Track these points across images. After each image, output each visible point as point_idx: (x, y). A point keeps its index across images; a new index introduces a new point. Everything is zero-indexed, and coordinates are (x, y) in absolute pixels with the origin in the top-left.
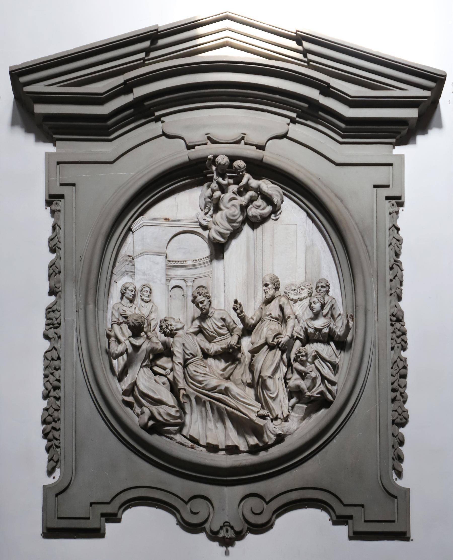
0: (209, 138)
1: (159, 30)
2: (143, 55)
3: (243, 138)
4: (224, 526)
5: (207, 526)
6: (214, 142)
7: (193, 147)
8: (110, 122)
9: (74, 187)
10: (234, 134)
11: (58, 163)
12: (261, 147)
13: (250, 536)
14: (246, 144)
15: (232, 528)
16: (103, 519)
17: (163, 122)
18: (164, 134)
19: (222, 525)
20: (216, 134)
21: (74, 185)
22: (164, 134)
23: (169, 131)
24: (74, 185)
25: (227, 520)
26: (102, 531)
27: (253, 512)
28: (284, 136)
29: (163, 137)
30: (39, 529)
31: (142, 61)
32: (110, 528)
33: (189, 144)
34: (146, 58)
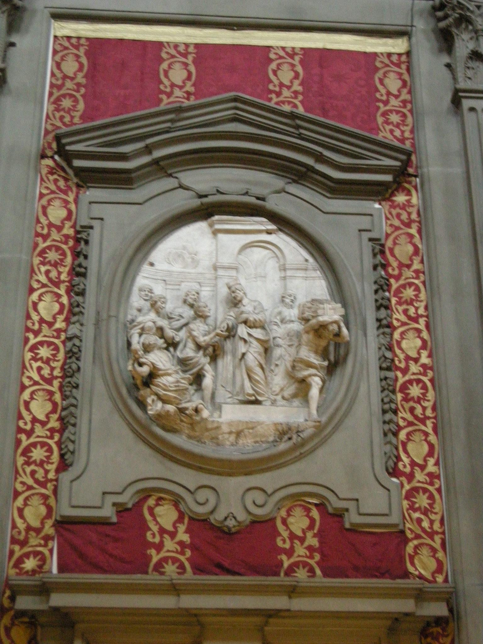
0: (218, 191)
8: (133, 175)
10: (242, 187)
15: (235, 518)
18: (181, 186)
22: (181, 186)
28: (284, 191)
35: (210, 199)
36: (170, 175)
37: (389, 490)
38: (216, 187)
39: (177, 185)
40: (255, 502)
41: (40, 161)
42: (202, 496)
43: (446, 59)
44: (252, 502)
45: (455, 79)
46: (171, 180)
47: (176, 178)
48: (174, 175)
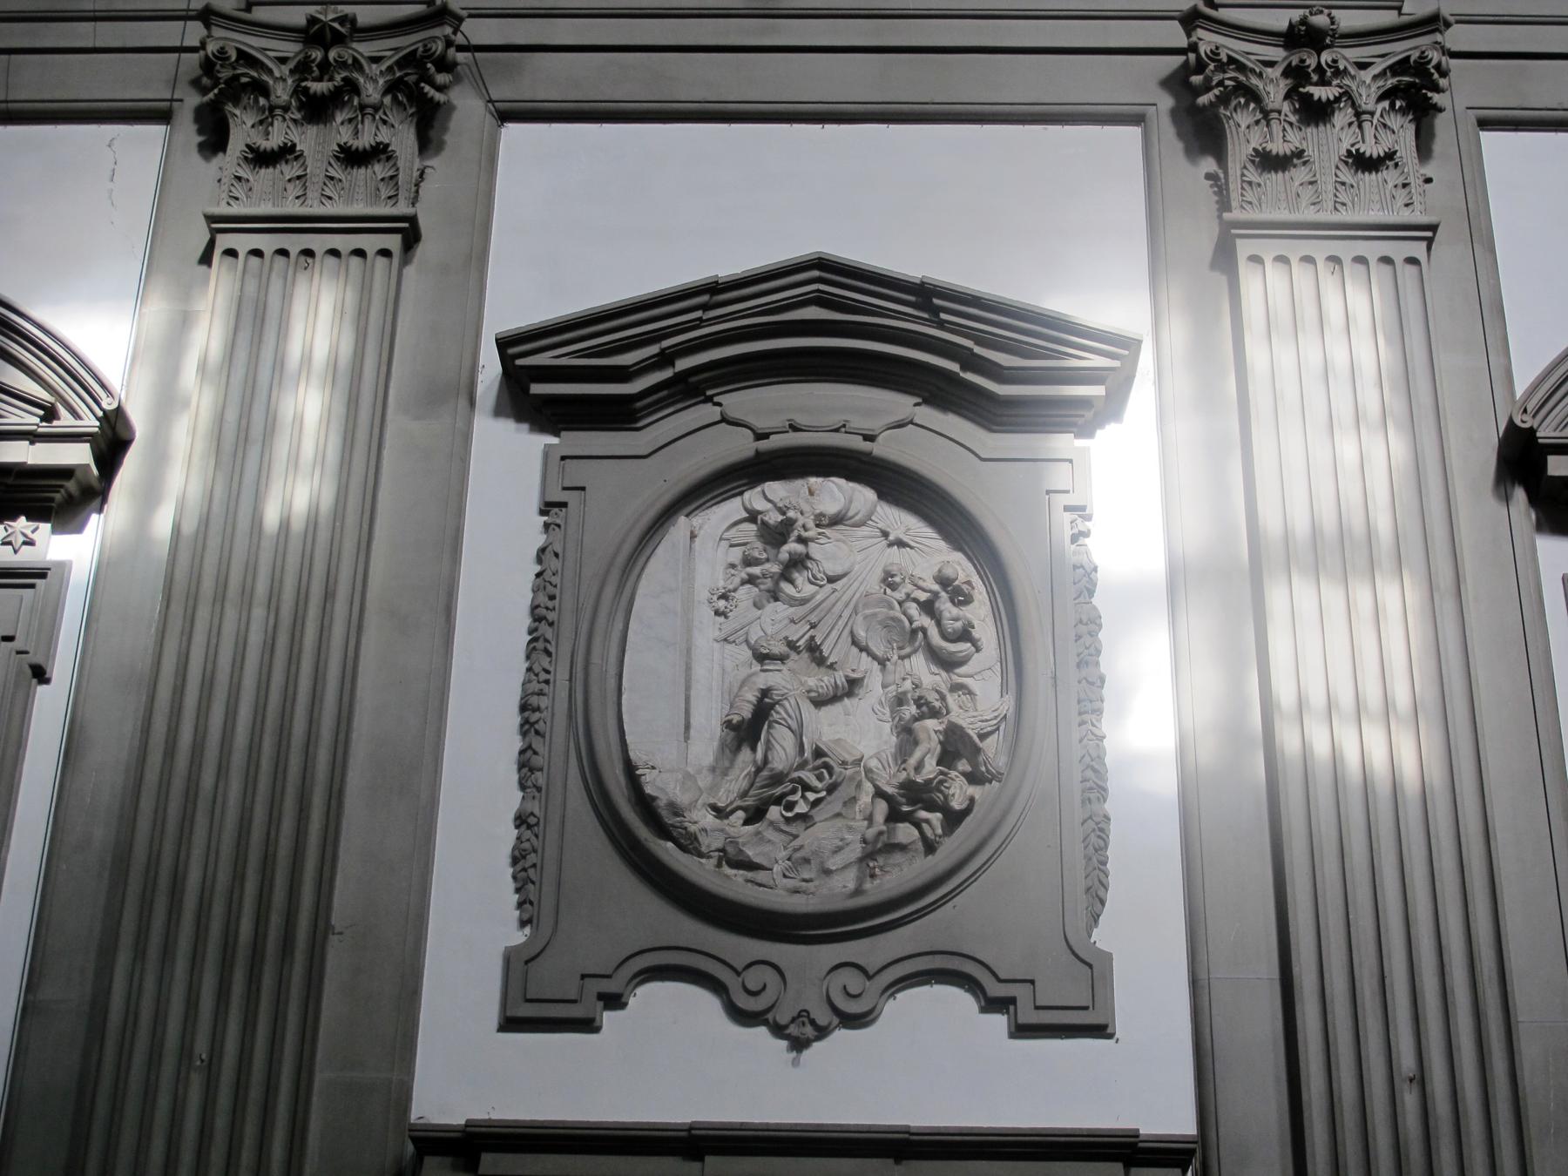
1: (720, 282)
2: (698, 314)
3: (844, 426)
4: (799, 1016)
5: (770, 1016)
6: (794, 428)
7: (765, 436)
9: (583, 492)
11: (563, 458)
12: (869, 438)
13: (841, 1036)
14: (846, 432)
16: (600, 1004)
17: (719, 404)
18: (724, 419)
19: (795, 1014)
20: (801, 420)
21: (583, 489)
22: (724, 419)
23: (733, 414)
24: (583, 489)
25: (806, 1008)
26: (597, 1024)
27: (848, 994)
29: (723, 424)
30: (493, 1016)
31: (698, 322)
32: (609, 1018)
33: (760, 431)
34: (704, 318)
35: (776, 442)
36: (709, 399)
37: (1090, 966)
38: (789, 420)
39: (718, 418)
40: (847, 987)
41: (50, 537)
42: (754, 978)
43: (1209, 164)
44: (841, 986)
45: (1224, 204)
46: (709, 407)
47: (719, 404)
48: (716, 399)
